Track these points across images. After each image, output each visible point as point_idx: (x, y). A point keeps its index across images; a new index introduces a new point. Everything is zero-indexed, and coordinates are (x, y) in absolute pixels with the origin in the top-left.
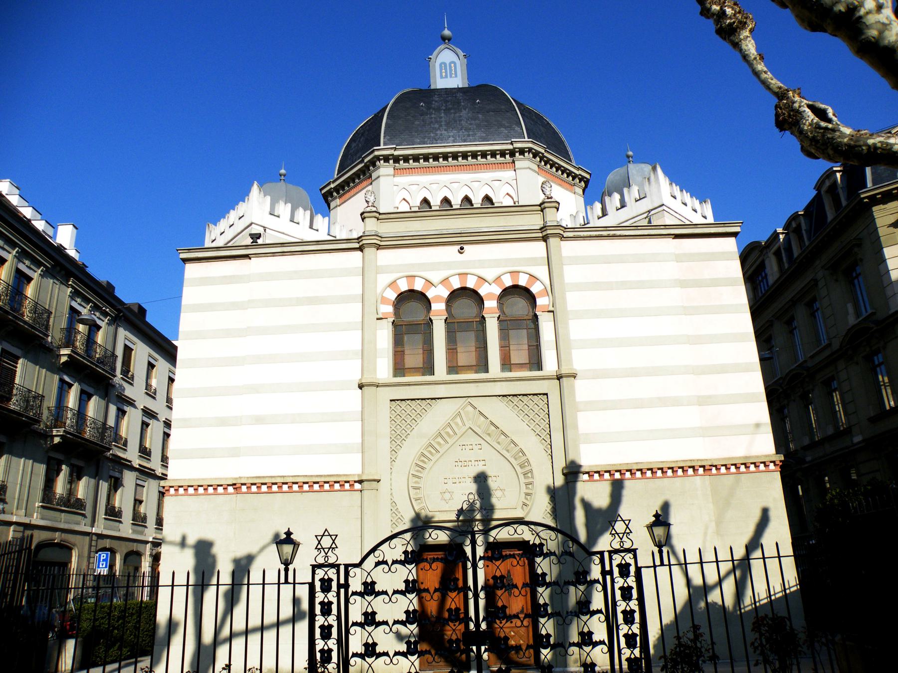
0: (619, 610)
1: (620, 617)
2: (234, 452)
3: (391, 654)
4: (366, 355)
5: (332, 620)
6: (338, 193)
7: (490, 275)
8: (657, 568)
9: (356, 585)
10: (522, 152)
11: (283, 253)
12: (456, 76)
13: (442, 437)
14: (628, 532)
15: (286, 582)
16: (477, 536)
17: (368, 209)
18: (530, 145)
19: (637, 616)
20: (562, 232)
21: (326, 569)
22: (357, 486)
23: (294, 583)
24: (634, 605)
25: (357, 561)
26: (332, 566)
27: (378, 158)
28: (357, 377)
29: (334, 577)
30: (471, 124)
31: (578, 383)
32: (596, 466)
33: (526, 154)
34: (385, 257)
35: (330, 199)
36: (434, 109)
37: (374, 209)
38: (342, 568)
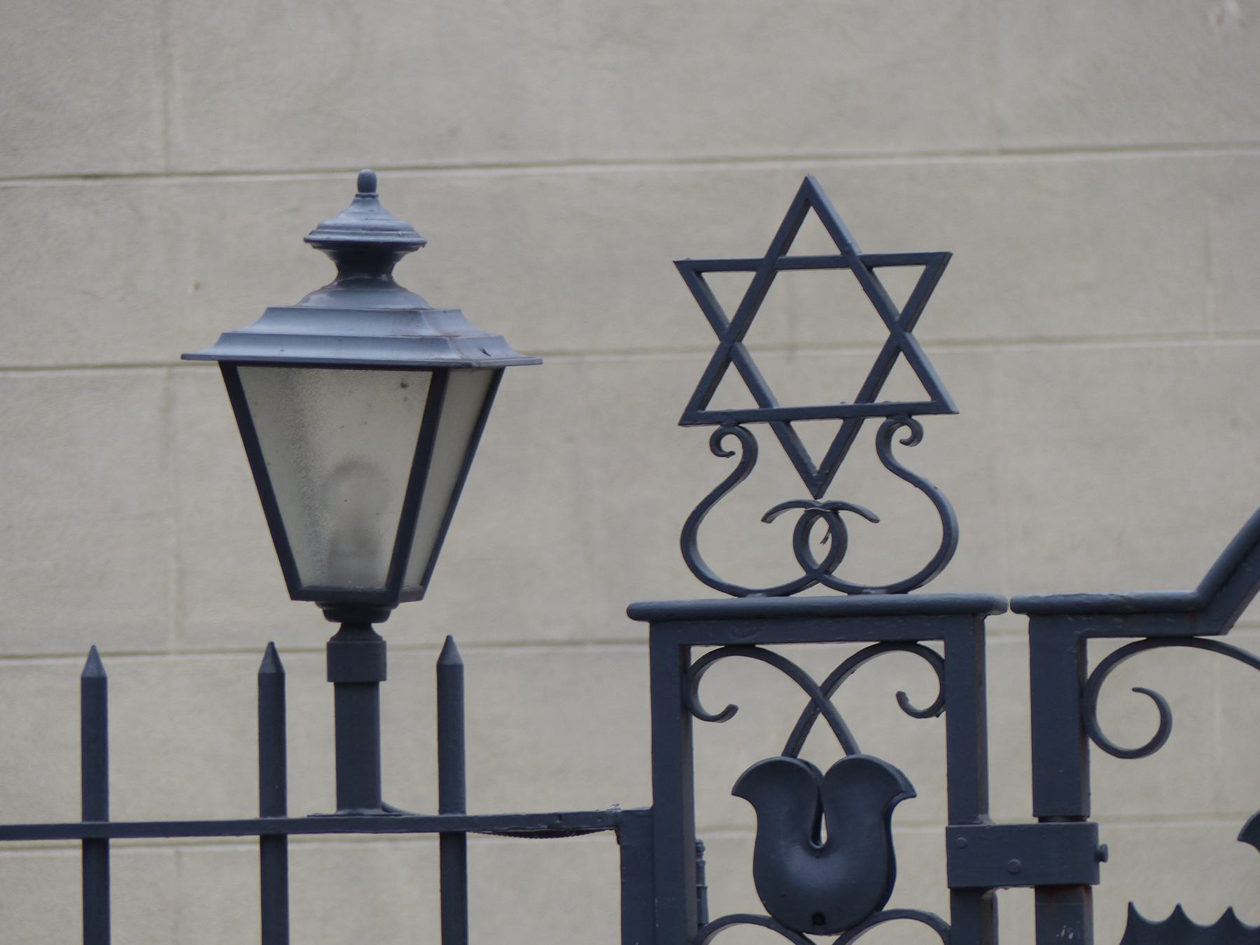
15: (360, 803)
21: (818, 658)
25: (1185, 581)
26: (889, 623)
29: (918, 752)
38: (1007, 651)
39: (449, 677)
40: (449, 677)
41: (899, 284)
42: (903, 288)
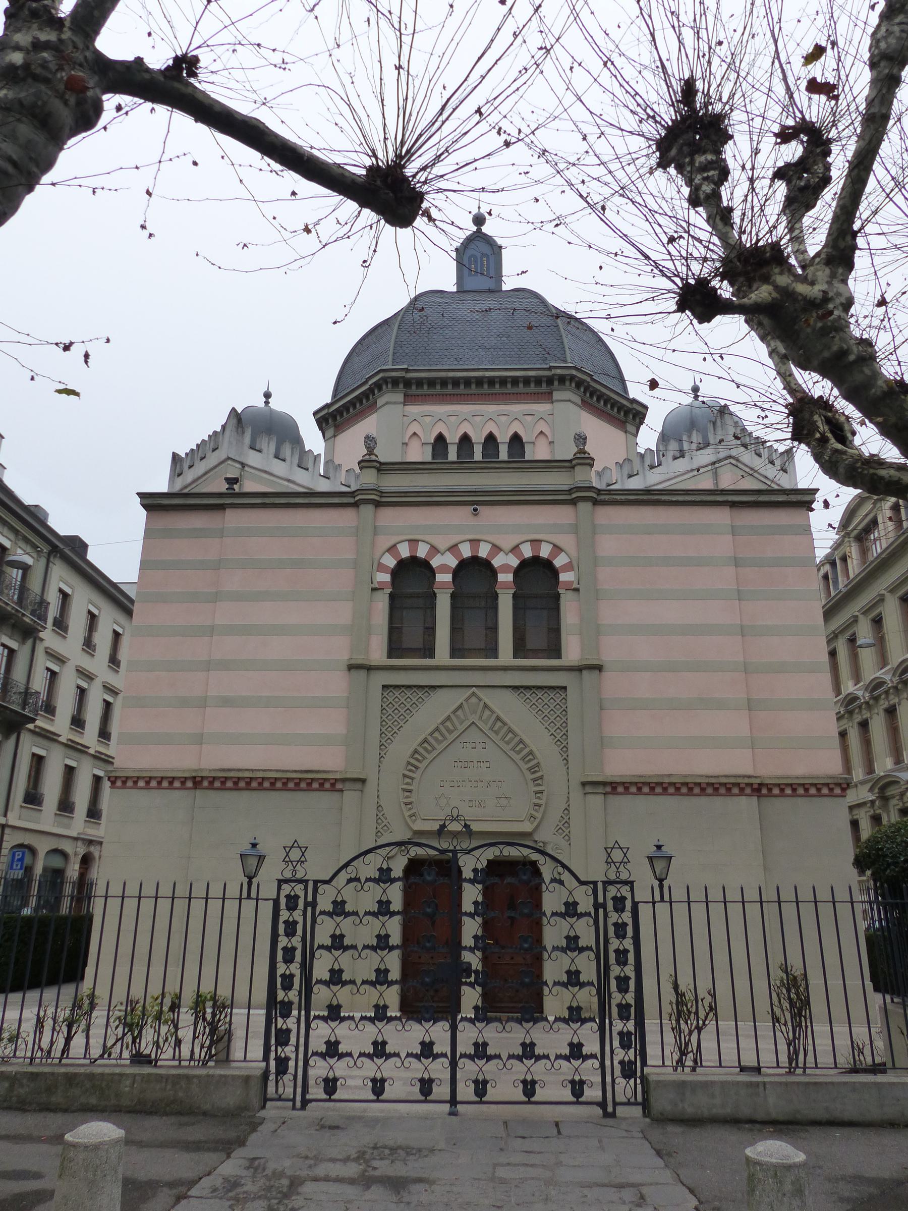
5: (296, 941)
9: (325, 903)
16: (459, 855)
21: (293, 884)
26: (300, 881)
29: (302, 894)
38: (311, 884)
39: (670, 887)
40: (670, 887)
42: (304, 850)
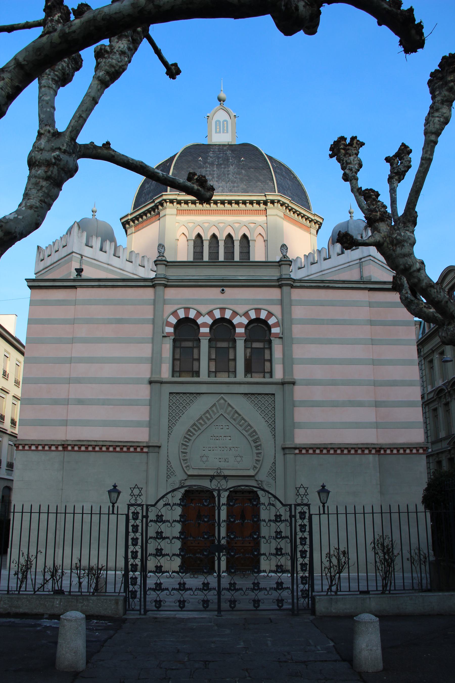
0: (298, 537)
1: (298, 541)
2: (65, 423)
3: (171, 555)
4: (155, 361)
6: (134, 222)
7: (241, 309)
8: (321, 516)
9: (152, 516)
10: (273, 202)
11: (99, 286)
12: (227, 132)
13: (203, 420)
14: (306, 494)
16: (221, 492)
17: (160, 258)
18: (279, 198)
19: (308, 541)
20: (292, 283)
21: (136, 507)
22: (145, 450)
23: (117, 514)
24: (306, 535)
25: (153, 504)
26: (139, 505)
27: (165, 200)
28: (147, 375)
29: (140, 512)
30: (236, 178)
31: (296, 388)
32: (304, 444)
33: (276, 204)
34: (171, 293)
35: (127, 226)
36: (209, 164)
37: (164, 259)
38: (145, 507)
41: (140, 489)
42: (140, 489)
